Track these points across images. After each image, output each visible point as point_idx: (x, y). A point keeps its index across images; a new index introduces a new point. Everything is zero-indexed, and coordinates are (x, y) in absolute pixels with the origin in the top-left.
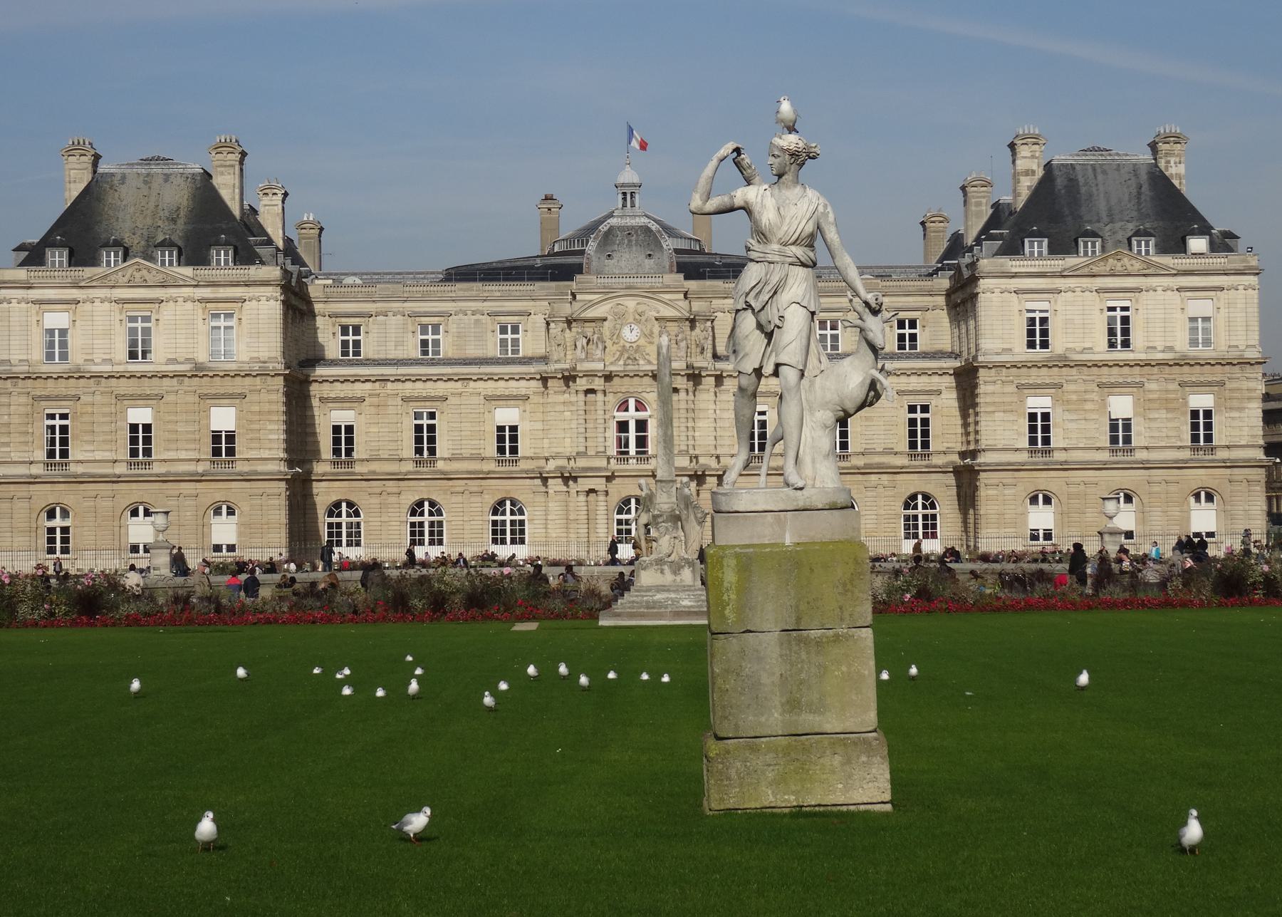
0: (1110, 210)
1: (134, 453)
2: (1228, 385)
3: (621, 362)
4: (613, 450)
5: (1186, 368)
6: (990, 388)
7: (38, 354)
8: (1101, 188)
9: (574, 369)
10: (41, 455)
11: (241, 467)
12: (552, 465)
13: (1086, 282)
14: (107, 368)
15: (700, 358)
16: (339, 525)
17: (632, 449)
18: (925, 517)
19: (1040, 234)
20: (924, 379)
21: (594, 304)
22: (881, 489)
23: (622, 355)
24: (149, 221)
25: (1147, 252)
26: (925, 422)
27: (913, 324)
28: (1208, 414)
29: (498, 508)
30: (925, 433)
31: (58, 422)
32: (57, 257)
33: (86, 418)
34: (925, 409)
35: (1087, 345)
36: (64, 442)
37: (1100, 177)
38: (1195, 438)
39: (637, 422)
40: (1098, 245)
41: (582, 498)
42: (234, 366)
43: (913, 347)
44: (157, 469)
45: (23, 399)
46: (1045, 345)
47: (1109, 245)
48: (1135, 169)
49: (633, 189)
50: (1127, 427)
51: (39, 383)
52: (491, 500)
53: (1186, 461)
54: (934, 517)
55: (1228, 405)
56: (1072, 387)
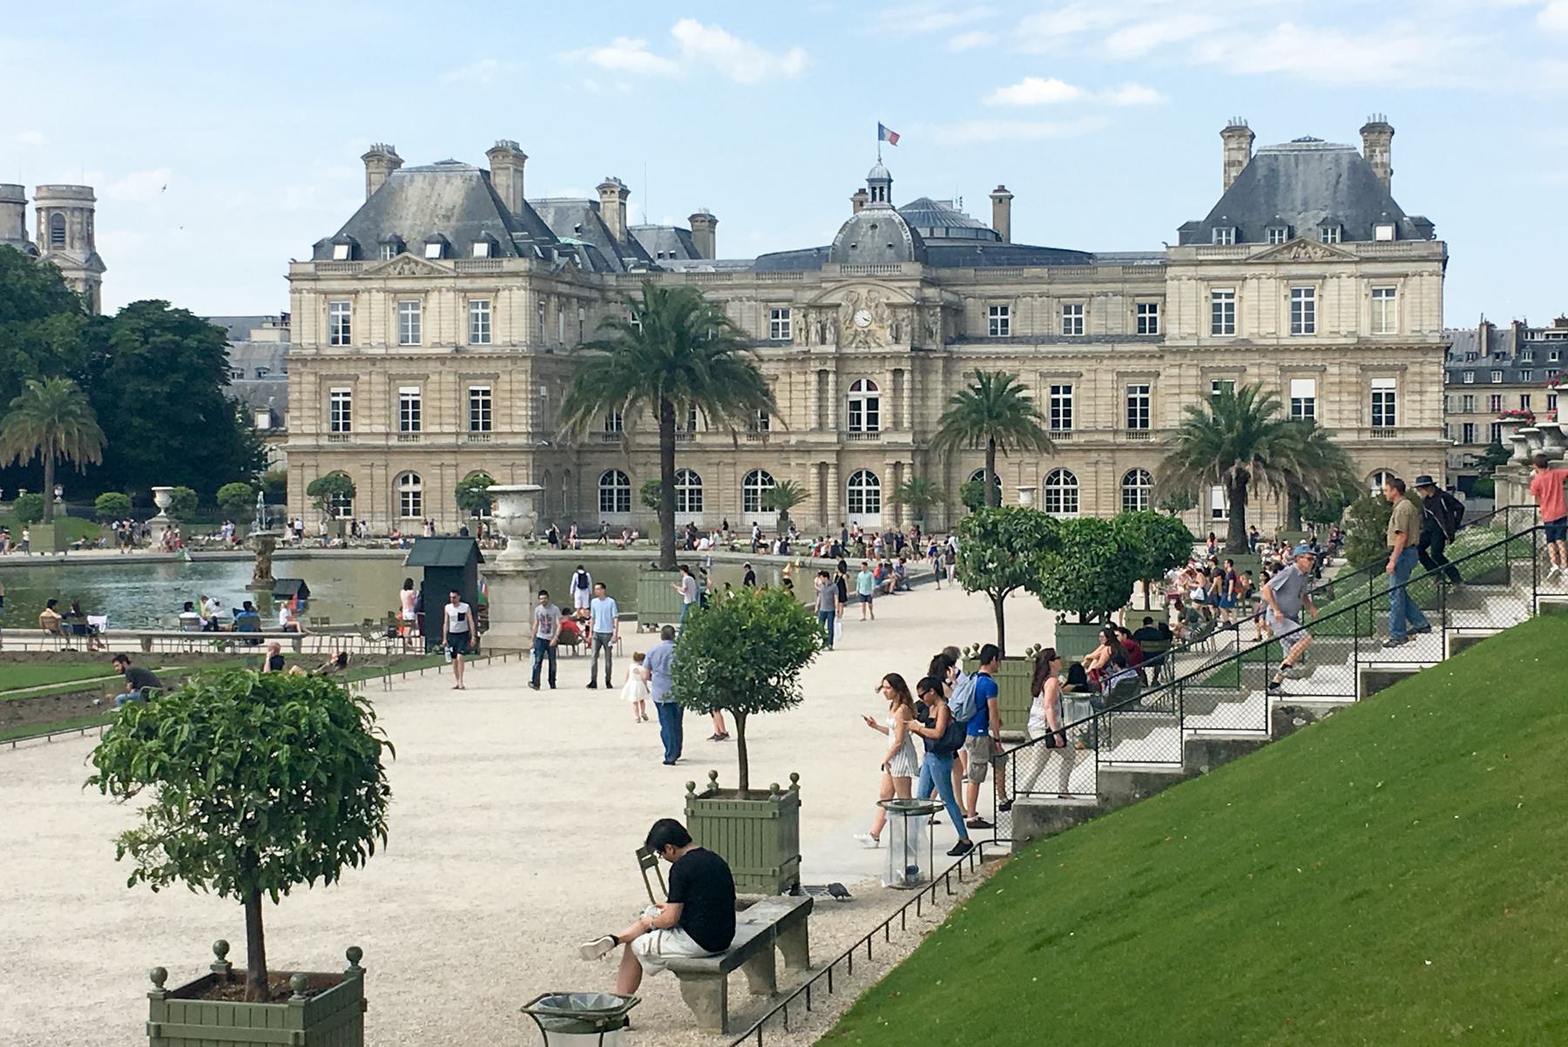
1: (405, 426)
2: (1412, 369)
4: (846, 427)
5: (1369, 354)
6: (1175, 371)
7: (324, 339)
8: (1301, 177)
10: (326, 428)
11: (493, 440)
12: (793, 440)
13: (1270, 270)
14: (383, 351)
15: (929, 341)
16: (611, 491)
17: (864, 426)
19: (1229, 224)
20: (1145, 362)
21: (829, 292)
22: (1101, 465)
25: (1334, 240)
26: (1145, 402)
27: (1153, 309)
28: (1390, 397)
29: (751, 478)
30: (1145, 413)
31: (341, 399)
32: (341, 252)
34: (1145, 390)
36: (346, 416)
37: (1301, 167)
38: (1377, 421)
39: (869, 400)
40: (1285, 233)
41: (814, 470)
42: (488, 350)
44: (422, 441)
45: (312, 378)
46: (1230, 329)
47: (1299, 233)
48: (1337, 161)
50: (1310, 410)
51: (325, 366)
52: (743, 471)
53: (1365, 443)
55: (1411, 387)
56: (1255, 370)
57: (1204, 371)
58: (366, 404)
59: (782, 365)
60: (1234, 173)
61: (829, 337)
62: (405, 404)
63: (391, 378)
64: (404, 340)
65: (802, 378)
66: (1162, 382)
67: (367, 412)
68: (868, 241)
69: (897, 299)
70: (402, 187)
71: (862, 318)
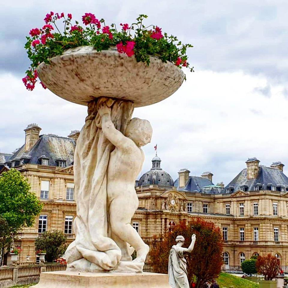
0: (279, 181)
3: (171, 211)
9: (162, 212)
10: (37, 231)
14: (62, 202)
18: (226, 258)
20: (227, 221)
23: (171, 208)
24: (65, 154)
27: (206, 207)
30: (226, 236)
33: (54, 219)
34: (226, 229)
35: (285, 215)
43: (206, 212)
49: (158, 162)
54: (228, 258)
57: (273, 224)
58: (54, 222)
59: (143, 215)
60: (256, 172)
61: (168, 207)
62: (66, 223)
63: (64, 212)
64: (68, 198)
65: (153, 220)
66: (231, 227)
67: (53, 225)
68: (162, 178)
69: (181, 197)
70: (50, 141)
71: (173, 202)
